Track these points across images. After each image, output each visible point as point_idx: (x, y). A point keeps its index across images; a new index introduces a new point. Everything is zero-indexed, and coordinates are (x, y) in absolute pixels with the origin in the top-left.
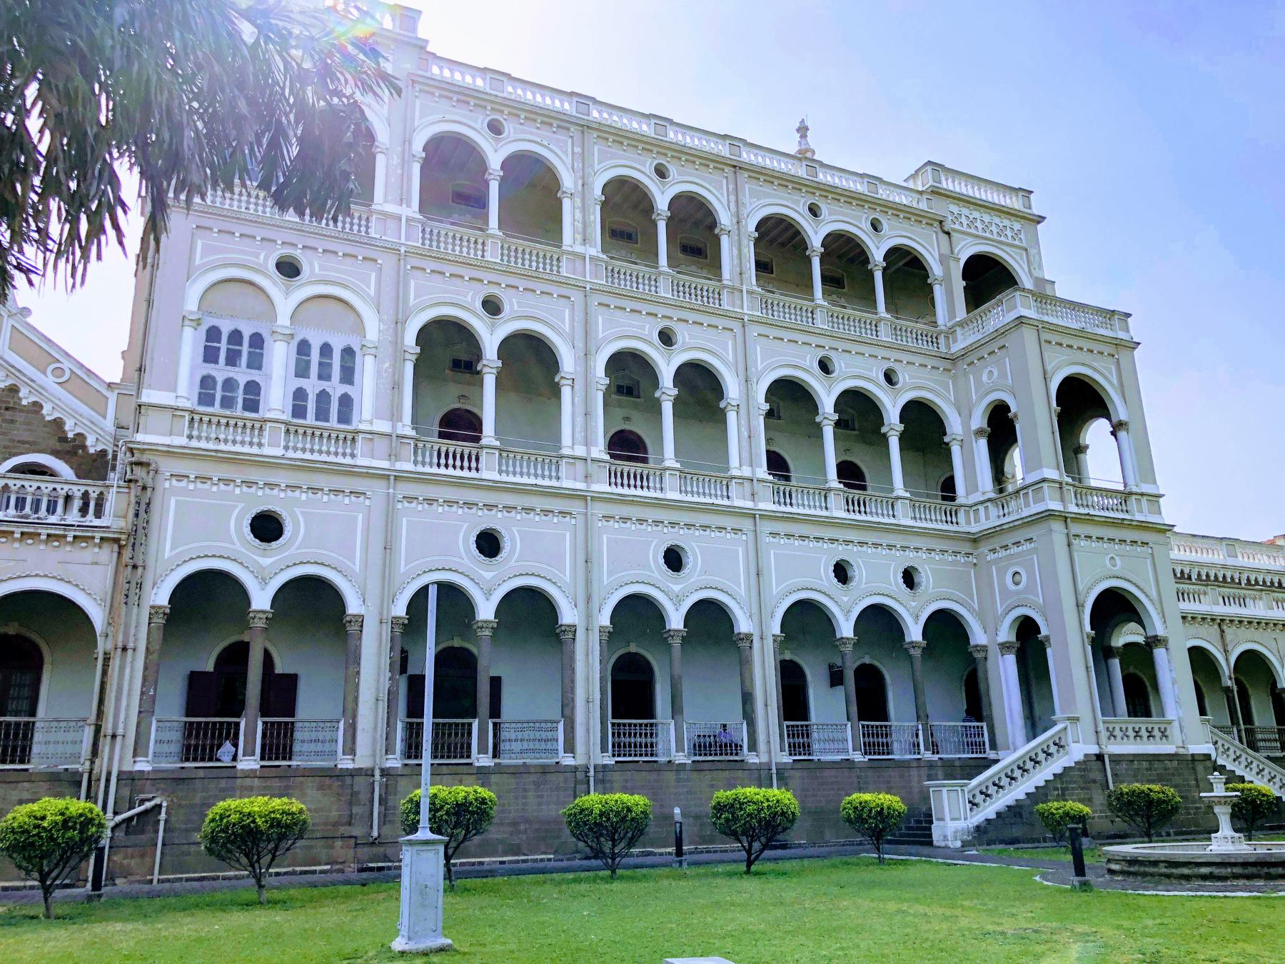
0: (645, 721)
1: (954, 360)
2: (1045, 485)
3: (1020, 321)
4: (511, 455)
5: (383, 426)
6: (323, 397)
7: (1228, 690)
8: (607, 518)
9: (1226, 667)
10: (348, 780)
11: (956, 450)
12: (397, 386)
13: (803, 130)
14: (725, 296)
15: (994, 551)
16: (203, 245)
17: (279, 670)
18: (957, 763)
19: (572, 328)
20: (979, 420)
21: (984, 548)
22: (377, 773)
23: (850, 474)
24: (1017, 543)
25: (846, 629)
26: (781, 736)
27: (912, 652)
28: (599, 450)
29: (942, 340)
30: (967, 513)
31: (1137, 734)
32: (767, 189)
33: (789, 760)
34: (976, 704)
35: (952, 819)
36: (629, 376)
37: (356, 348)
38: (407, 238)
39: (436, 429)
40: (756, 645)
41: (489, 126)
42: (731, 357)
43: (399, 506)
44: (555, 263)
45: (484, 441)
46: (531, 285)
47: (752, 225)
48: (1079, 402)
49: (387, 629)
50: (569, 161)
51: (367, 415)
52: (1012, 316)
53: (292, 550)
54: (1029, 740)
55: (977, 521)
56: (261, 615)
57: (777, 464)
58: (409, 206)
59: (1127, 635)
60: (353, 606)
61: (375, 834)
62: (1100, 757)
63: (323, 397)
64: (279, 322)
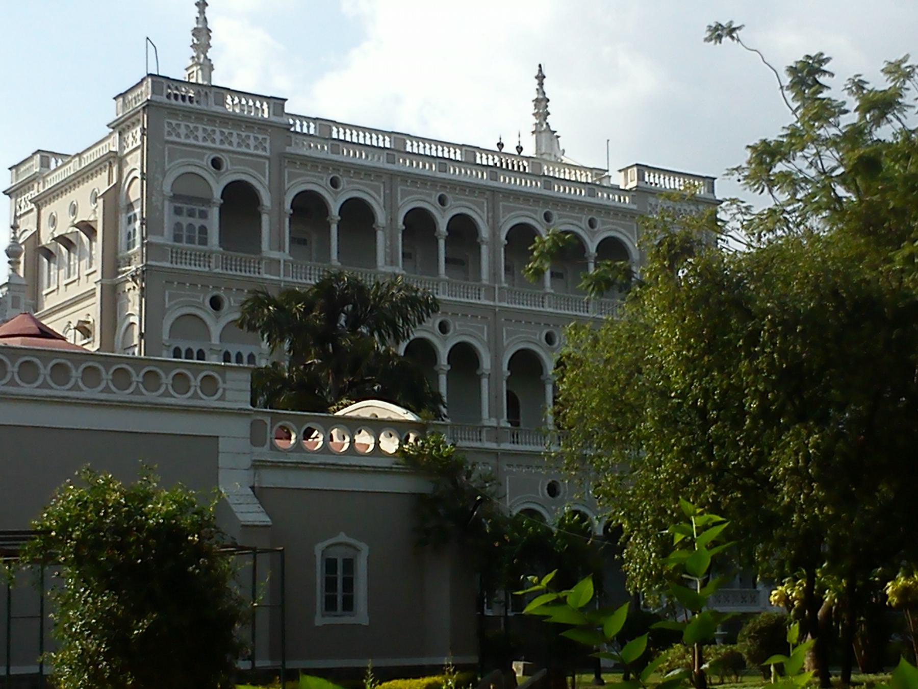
13: (540, 66)
16: (169, 293)
41: (332, 179)
42: (485, 338)
50: (381, 201)
64: (213, 342)
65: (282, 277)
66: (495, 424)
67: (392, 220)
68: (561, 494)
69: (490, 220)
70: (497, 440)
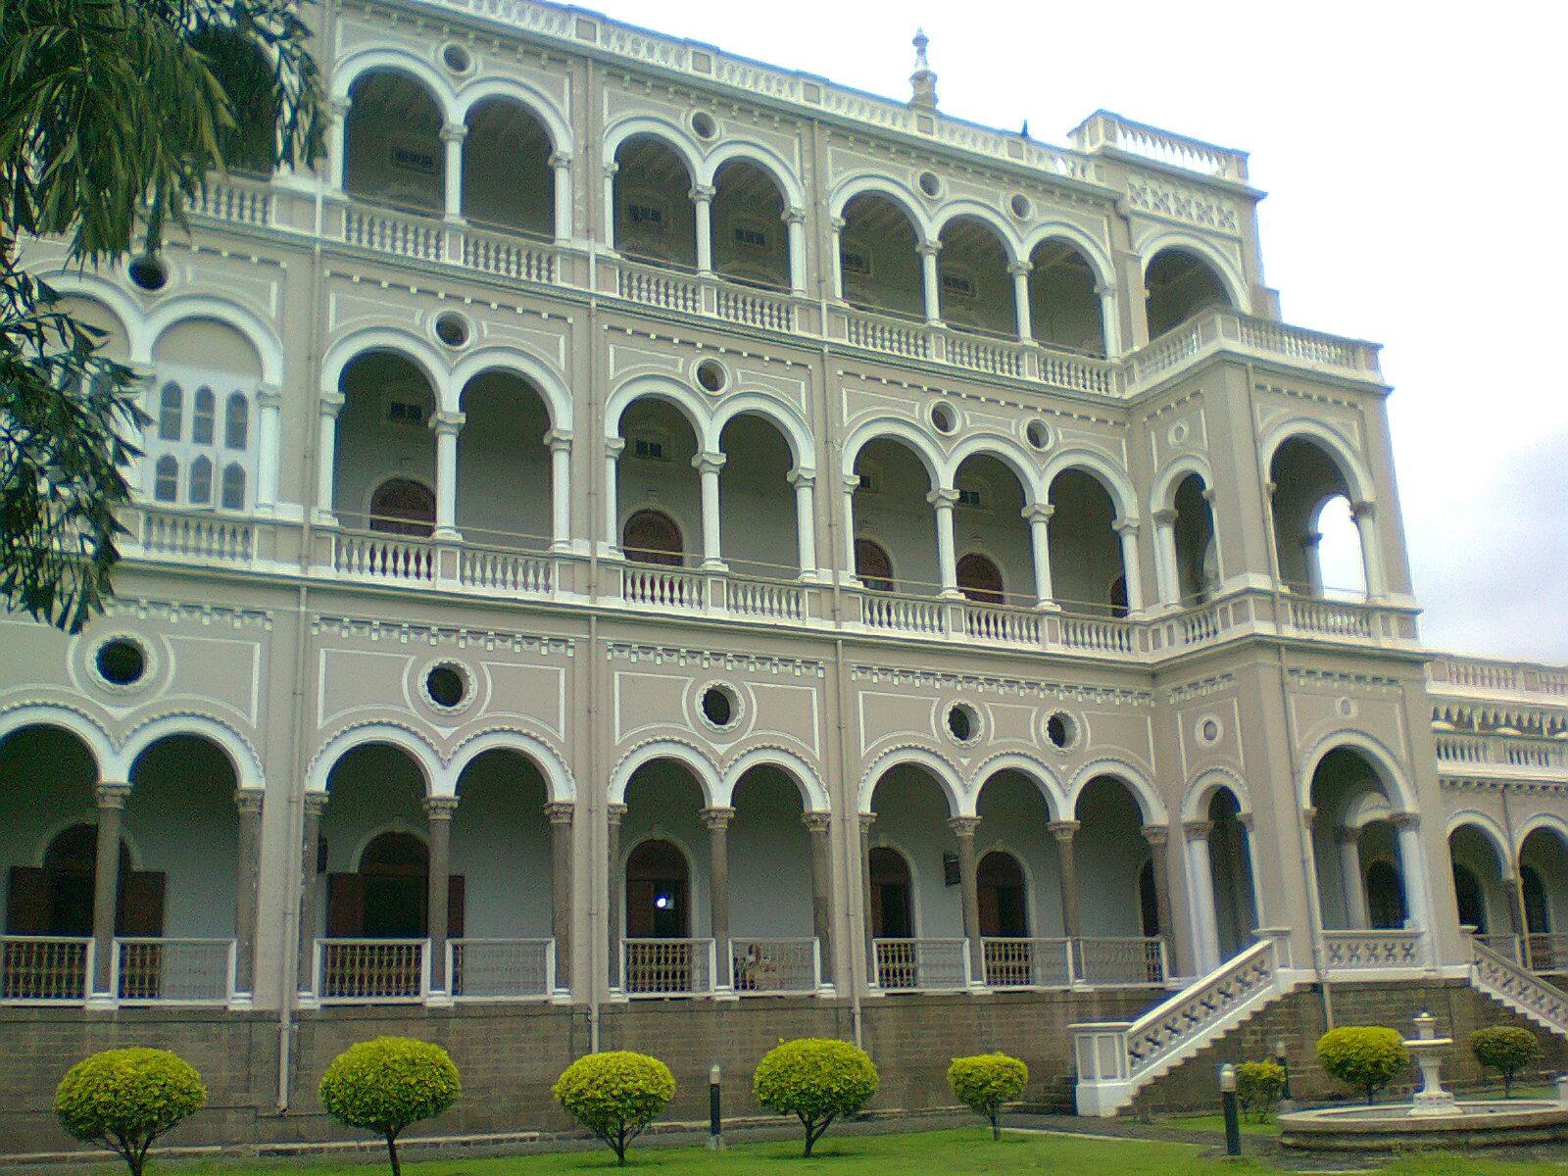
0: (672, 941)
1: (1129, 409)
2: (1251, 599)
3: (1223, 359)
4: (480, 555)
5: (291, 513)
6: (202, 467)
7: (1511, 885)
8: (620, 647)
9: (1510, 847)
10: (244, 1028)
11: (1130, 544)
12: (311, 456)
13: (920, 42)
14: (796, 315)
15: (1178, 690)
17: (138, 865)
18: (1121, 996)
19: (570, 361)
20: (1160, 501)
21: (1166, 687)
22: (286, 1020)
23: (978, 575)
24: (1211, 681)
25: (966, 806)
26: (869, 958)
27: (1060, 837)
28: (609, 548)
29: (1113, 379)
30: (1143, 634)
31: (1373, 954)
32: (858, 154)
33: (881, 993)
34: (1152, 911)
35: (1106, 1077)
36: (654, 436)
37: (249, 394)
38: (324, 231)
39: (367, 516)
40: (835, 828)
43: (315, 631)
44: (544, 265)
45: (438, 535)
46: (508, 300)
47: (836, 211)
48: (1305, 475)
49: (297, 811)
51: (264, 499)
52: (1211, 348)
53: (160, 695)
54: (1224, 958)
55: (1157, 645)
56: (115, 791)
57: (872, 561)
58: (326, 179)
59: (1367, 812)
60: (249, 779)
61: (283, 1103)
62: (1316, 988)
63: (202, 467)
65: (317, 234)
66: (829, 582)
67: (590, 148)
68: (981, 732)
69: (808, 176)
70: (834, 615)
